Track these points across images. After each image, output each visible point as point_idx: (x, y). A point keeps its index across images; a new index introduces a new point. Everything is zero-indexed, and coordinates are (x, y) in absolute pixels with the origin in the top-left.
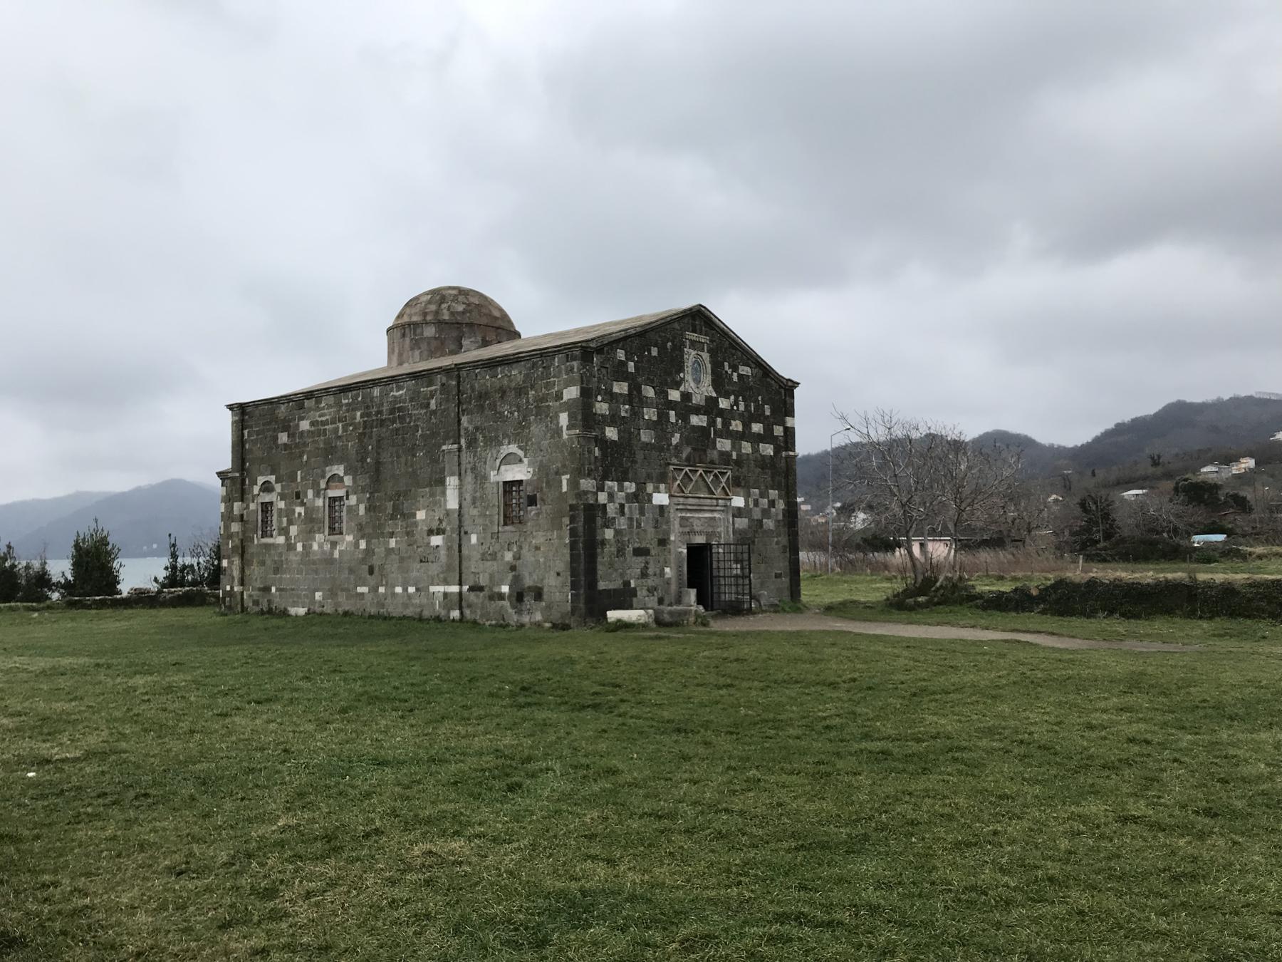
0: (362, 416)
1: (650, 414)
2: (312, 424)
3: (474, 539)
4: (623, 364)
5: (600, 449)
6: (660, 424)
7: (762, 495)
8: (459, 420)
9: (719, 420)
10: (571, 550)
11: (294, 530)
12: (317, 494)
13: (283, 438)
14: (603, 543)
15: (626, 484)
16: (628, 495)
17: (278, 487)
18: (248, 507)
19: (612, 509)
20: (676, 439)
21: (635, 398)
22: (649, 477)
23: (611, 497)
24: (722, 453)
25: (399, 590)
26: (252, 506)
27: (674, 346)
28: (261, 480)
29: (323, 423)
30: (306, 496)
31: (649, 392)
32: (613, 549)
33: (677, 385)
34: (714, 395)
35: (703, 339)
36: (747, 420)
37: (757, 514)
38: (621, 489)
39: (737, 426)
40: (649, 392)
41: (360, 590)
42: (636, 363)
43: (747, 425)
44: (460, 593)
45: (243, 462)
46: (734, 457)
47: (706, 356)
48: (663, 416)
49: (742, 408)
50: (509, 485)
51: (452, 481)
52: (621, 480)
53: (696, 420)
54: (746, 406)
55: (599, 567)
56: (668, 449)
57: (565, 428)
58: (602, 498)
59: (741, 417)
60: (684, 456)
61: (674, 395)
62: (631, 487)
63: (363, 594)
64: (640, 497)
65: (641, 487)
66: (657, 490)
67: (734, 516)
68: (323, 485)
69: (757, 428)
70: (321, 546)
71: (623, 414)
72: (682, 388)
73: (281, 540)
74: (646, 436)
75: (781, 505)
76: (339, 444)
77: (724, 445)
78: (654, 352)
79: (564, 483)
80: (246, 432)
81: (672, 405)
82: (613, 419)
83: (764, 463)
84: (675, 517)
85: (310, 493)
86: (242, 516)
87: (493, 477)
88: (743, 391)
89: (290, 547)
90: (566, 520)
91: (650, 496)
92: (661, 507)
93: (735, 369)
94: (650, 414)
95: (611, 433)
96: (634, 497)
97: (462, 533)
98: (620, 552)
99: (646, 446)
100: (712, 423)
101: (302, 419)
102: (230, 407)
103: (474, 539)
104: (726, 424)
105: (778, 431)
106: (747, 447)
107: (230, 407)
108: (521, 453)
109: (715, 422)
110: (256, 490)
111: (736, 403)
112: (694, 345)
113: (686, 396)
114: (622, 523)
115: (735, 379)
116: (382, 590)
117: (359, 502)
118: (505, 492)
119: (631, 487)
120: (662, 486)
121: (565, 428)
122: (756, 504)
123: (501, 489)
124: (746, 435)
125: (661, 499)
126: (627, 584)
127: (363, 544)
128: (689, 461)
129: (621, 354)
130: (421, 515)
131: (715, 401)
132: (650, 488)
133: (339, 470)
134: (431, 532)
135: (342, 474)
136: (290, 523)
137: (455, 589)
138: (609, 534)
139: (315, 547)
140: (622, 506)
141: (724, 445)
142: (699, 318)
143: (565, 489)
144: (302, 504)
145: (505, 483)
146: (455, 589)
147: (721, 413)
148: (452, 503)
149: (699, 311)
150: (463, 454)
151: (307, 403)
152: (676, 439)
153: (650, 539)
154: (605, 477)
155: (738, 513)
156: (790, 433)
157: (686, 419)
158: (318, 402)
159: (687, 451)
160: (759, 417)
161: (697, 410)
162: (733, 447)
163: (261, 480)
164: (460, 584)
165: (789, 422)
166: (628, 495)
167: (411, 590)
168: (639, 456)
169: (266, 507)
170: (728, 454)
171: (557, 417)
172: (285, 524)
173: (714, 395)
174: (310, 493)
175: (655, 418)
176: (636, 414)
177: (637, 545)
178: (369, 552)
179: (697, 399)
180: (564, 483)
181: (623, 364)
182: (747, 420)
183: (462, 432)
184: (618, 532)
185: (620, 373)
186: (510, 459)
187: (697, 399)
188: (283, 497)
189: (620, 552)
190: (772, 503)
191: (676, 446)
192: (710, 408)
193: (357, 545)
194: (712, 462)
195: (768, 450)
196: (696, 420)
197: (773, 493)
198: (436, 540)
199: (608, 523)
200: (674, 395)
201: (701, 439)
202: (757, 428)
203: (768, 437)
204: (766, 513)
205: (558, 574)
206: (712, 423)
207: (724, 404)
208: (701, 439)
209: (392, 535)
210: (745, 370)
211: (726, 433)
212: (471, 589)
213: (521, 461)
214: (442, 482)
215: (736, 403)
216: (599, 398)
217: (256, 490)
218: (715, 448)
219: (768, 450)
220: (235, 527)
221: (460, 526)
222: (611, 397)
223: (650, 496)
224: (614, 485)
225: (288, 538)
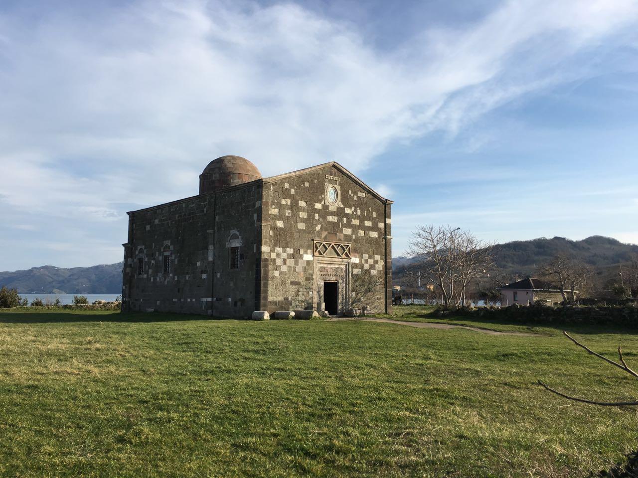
0: (178, 217)
1: (303, 215)
2: (159, 221)
3: (219, 275)
4: (289, 190)
5: (273, 232)
6: (309, 221)
7: (370, 257)
8: (215, 218)
9: (345, 219)
10: (256, 281)
11: (150, 271)
12: (160, 255)
13: (148, 228)
14: (273, 277)
15: (288, 249)
16: (288, 254)
17: (145, 251)
18: (133, 261)
19: (279, 262)
20: (318, 228)
21: (294, 206)
22: (302, 246)
23: (278, 255)
24: (346, 236)
25: (189, 300)
26: (135, 260)
27: (319, 182)
28: (139, 248)
29: (164, 220)
30: (155, 255)
31: (302, 204)
32: (279, 281)
33: (319, 201)
34: (342, 206)
35: (336, 178)
36: (362, 219)
37: (366, 267)
38: (284, 251)
39: (356, 222)
40: (302, 204)
41: (174, 300)
42: (296, 190)
43: (362, 222)
44: (212, 301)
45: (133, 240)
46: (354, 237)
47: (338, 187)
48: (311, 217)
49: (359, 213)
50: (234, 250)
51: (211, 247)
52: (284, 248)
53: (330, 218)
54: (361, 212)
55: (269, 289)
56: (313, 233)
57: (256, 221)
58: (273, 256)
59: (358, 217)
60: (323, 236)
61: (318, 206)
62: (290, 251)
63: (175, 302)
64: (296, 256)
65: (297, 251)
66: (306, 253)
67: (353, 268)
68: (162, 250)
69: (368, 223)
70: (160, 279)
71: (287, 215)
72: (323, 203)
73: (145, 276)
74: (301, 226)
75: (382, 263)
76: (169, 230)
77: (348, 231)
78: (307, 185)
79: (255, 248)
80: (134, 225)
81: (318, 211)
82: (280, 217)
83: (371, 241)
84: (317, 267)
85: (157, 254)
86: (131, 265)
87: (228, 245)
88: (360, 203)
89: (148, 279)
90: (254, 266)
91: (302, 255)
92: (308, 262)
93: (355, 193)
94: (303, 215)
95: (280, 224)
96: (292, 256)
97: (214, 273)
98: (283, 283)
99: (300, 231)
100: (340, 220)
101: (156, 219)
102: (128, 213)
103: (219, 275)
104: (349, 222)
105: (381, 225)
106: (361, 233)
107: (128, 213)
108: (238, 233)
110: (137, 252)
111: (356, 210)
112: (330, 181)
113: (326, 207)
114: (284, 269)
115: (355, 198)
116: (182, 300)
117: (175, 258)
118: (232, 252)
119: (290, 251)
120: (309, 251)
121: (256, 221)
122: (366, 262)
123: (230, 251)
124: (361, 226)
125: (308, 257)
126: (286, 299)
127: (176, 278)
128: (325, 239)
129: (287, 186)
130: (199, 264)
131: (343, 209)
132: (302, 252)
133: (168, 242)
134: (202, 272)
135: (169, 245)
136: (149, 268)
137: (210, 299)
138: (277, 273)
139: (158, 279)
140: (285, 261)
141: (348, 231)
142: (336, 169)
143: (255, 251)
144: (154, 259)
145: (232, 248)
146: (210, 299)
147: (347, 215)
148: (211, 259)
149: (334, 166)
150: (216, 234)
151: (158, 211)
152: (318, 228)
153: (301, 278)
154: (275, 245)
155: (355, 266)
156: (387, 228)
157: (324, 218)
158: (162, 211)
159: (324, 234)
160: (369, 218)
161: (332, 214)
162: (353, 233)
163: (139, 248)
164: (212, 297)
165: (388, 221)
166: (288, 254)
167: (194, 300)
168: (296, 235)
169: (141, 260)
170: (351, 236)
171: (253, 216)
172: (147, 269)
173: (342, 206)
174: (157, 254)
175: (305, 217)
176: (295, 215)
177: (293, 280)
178: (178, 281)
179: (332, 208)
180: (255, 248)
181: (289, 190)
182: (362, 219)
183: (216, 224)
184: (281, 273)
185: (286, 194)
186: (235, 237)
187: (332, 208)
188: (147, 255)
189: (283, 283)
190: (376, 262)
191: (318, 232)
192: (340, 213)
193: (174, 278)
194: (340, 240)
195: (374, 235)
196: (330, 218)
197: (377, 257)
198: (204, 276)
199: (277, 268)
200: (318, 206)
201: (334, 229)
202: (368, 223)
203: (375, 228)
204: (372, 267)
205: (251, 293)
206: (340, 220)
207: (348, 211)
208: (334, 229)
209: (187, 273)
210: (362, 194)
211: (349, 225)
212: (217, 300)
213: (238, 238)
214: (207, 248)
215: (356, 210)
216: (273, 206)
217: (137, 252)
218: (342, 232)
219: (374, 235)
220: (128, 270)
221: (213, 269)
222: (280, 206)
223: (301, 257)
225: (148, 275)
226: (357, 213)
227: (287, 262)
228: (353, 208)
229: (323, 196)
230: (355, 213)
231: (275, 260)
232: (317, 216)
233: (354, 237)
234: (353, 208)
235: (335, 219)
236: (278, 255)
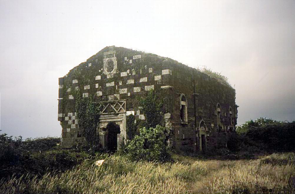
23: (70, 118)
27: (99, 60)
36: (136, 79)
53: (108, 85)
61: (98, 78)
69: (144, 80)
109: (118, 84)
113: (104, 77)
115: (131, 62)
140: (74, 121)
141: (124, 91)
147: (122, 79)
161: (110, 81)
162: (128, 91)
192: (117, 78)
196: (108, 85)
200: (98, 78)
202: (144, 80)
211: (125, 85)
215: (131, 72)
224: (72, 114)
226: (132, 74)
227: (75, 121)
228: (128, 71)
229: (102, 69)
230: (130, 74)
231: (67, 121)
232: (97, 86)
233: (129, 94)
234: (128, 71)
235: (113, 84)
236: (70, 118)
